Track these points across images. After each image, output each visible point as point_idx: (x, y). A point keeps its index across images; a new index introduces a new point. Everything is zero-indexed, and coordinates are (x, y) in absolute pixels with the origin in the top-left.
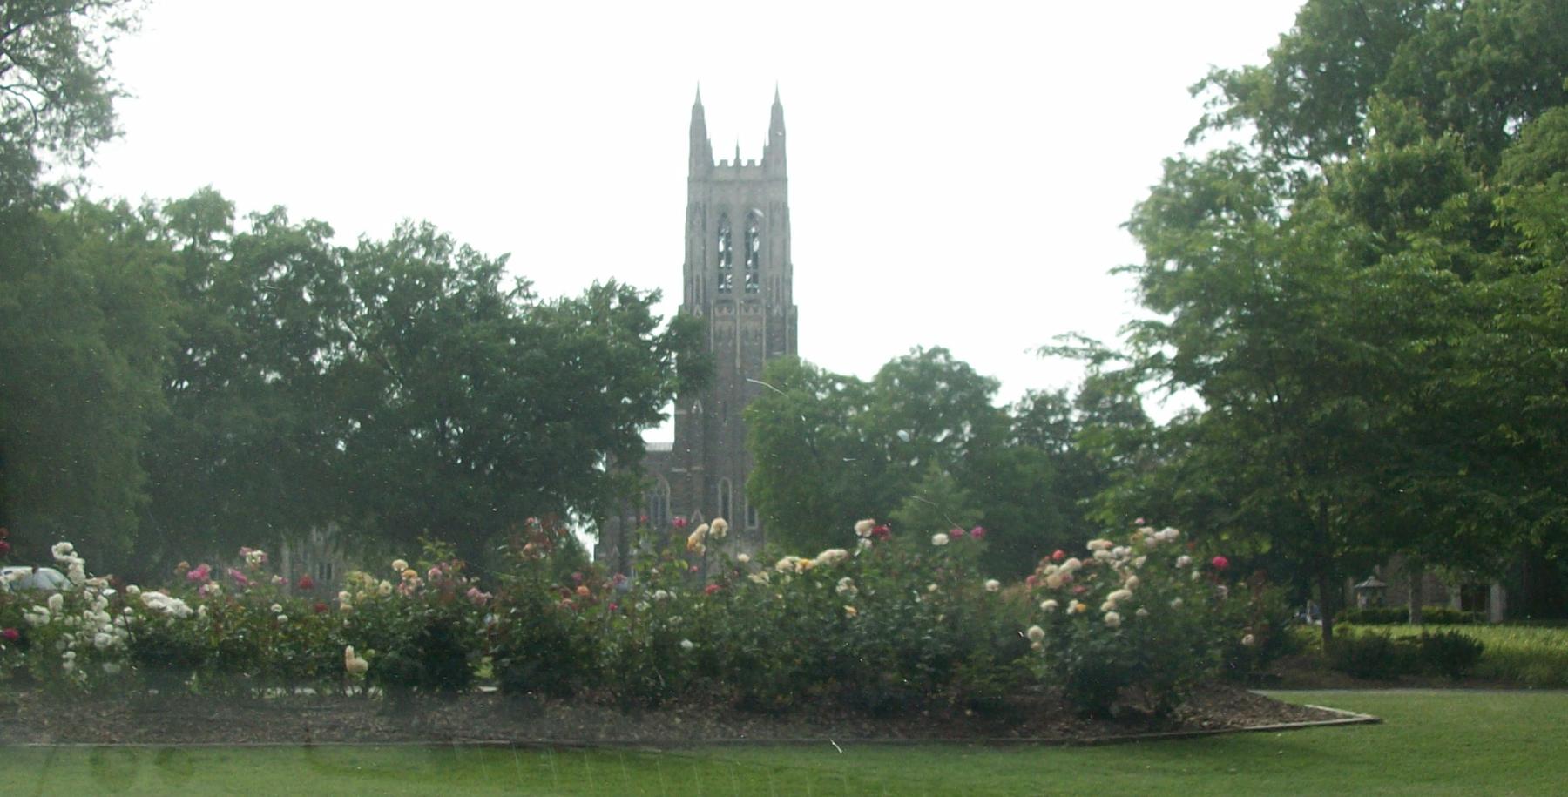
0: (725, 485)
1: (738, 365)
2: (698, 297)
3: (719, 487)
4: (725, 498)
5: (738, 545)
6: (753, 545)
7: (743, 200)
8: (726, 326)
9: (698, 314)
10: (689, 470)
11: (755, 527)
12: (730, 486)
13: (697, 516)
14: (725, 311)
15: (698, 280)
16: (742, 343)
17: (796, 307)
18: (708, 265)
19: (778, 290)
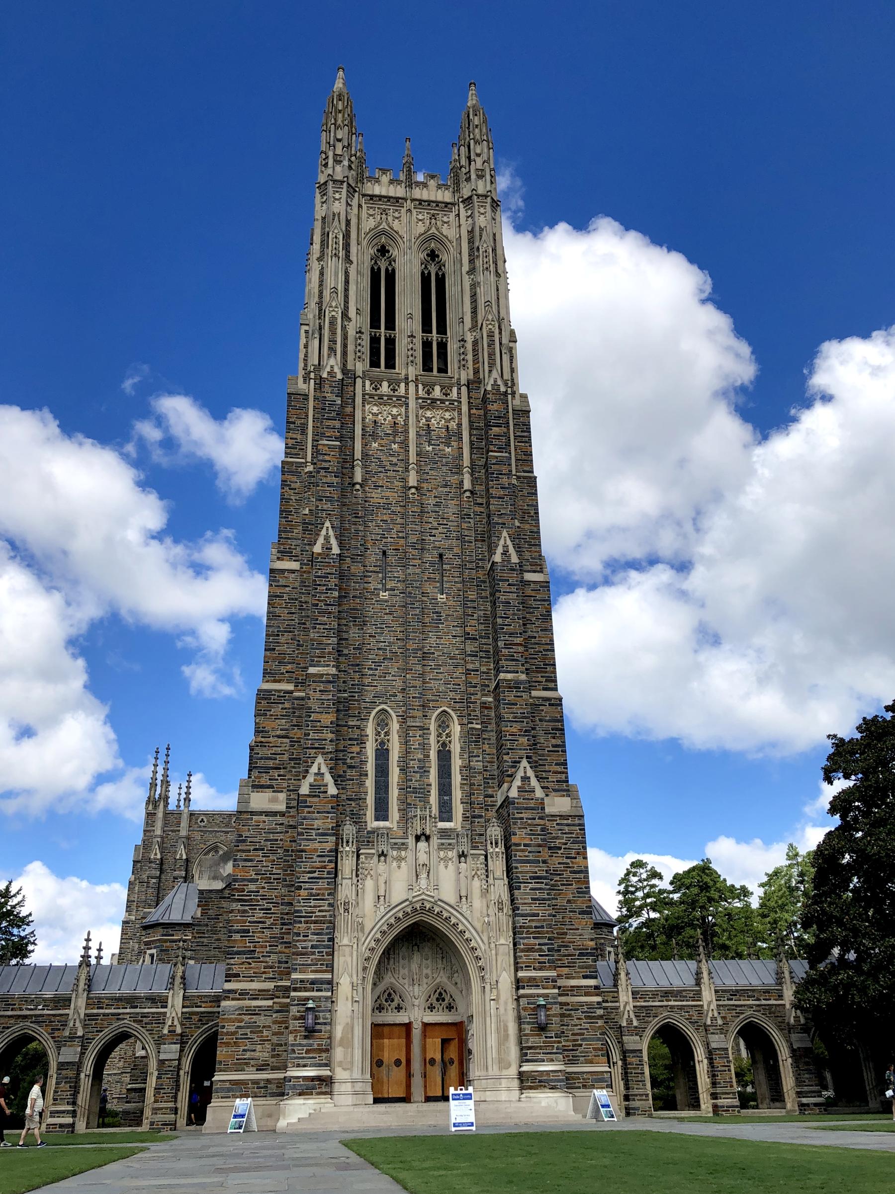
0: (383, 722)
1: (412, 480)
2: (332, 350)
3: (370, 730)
4: (382, 754)
5: (423, 858)
6: (462, 855)
7: (421, 228)
8: (386, 415)
9: (331, 373)
10: (301, 683)
11: (456, 823)
12: (395, 726)
13: (319, 774)
14: (385, 388)
15: (333, 323)
16: (419, 445)
17: (524, 397)
18: (352, 313)
19: (491, 355)
